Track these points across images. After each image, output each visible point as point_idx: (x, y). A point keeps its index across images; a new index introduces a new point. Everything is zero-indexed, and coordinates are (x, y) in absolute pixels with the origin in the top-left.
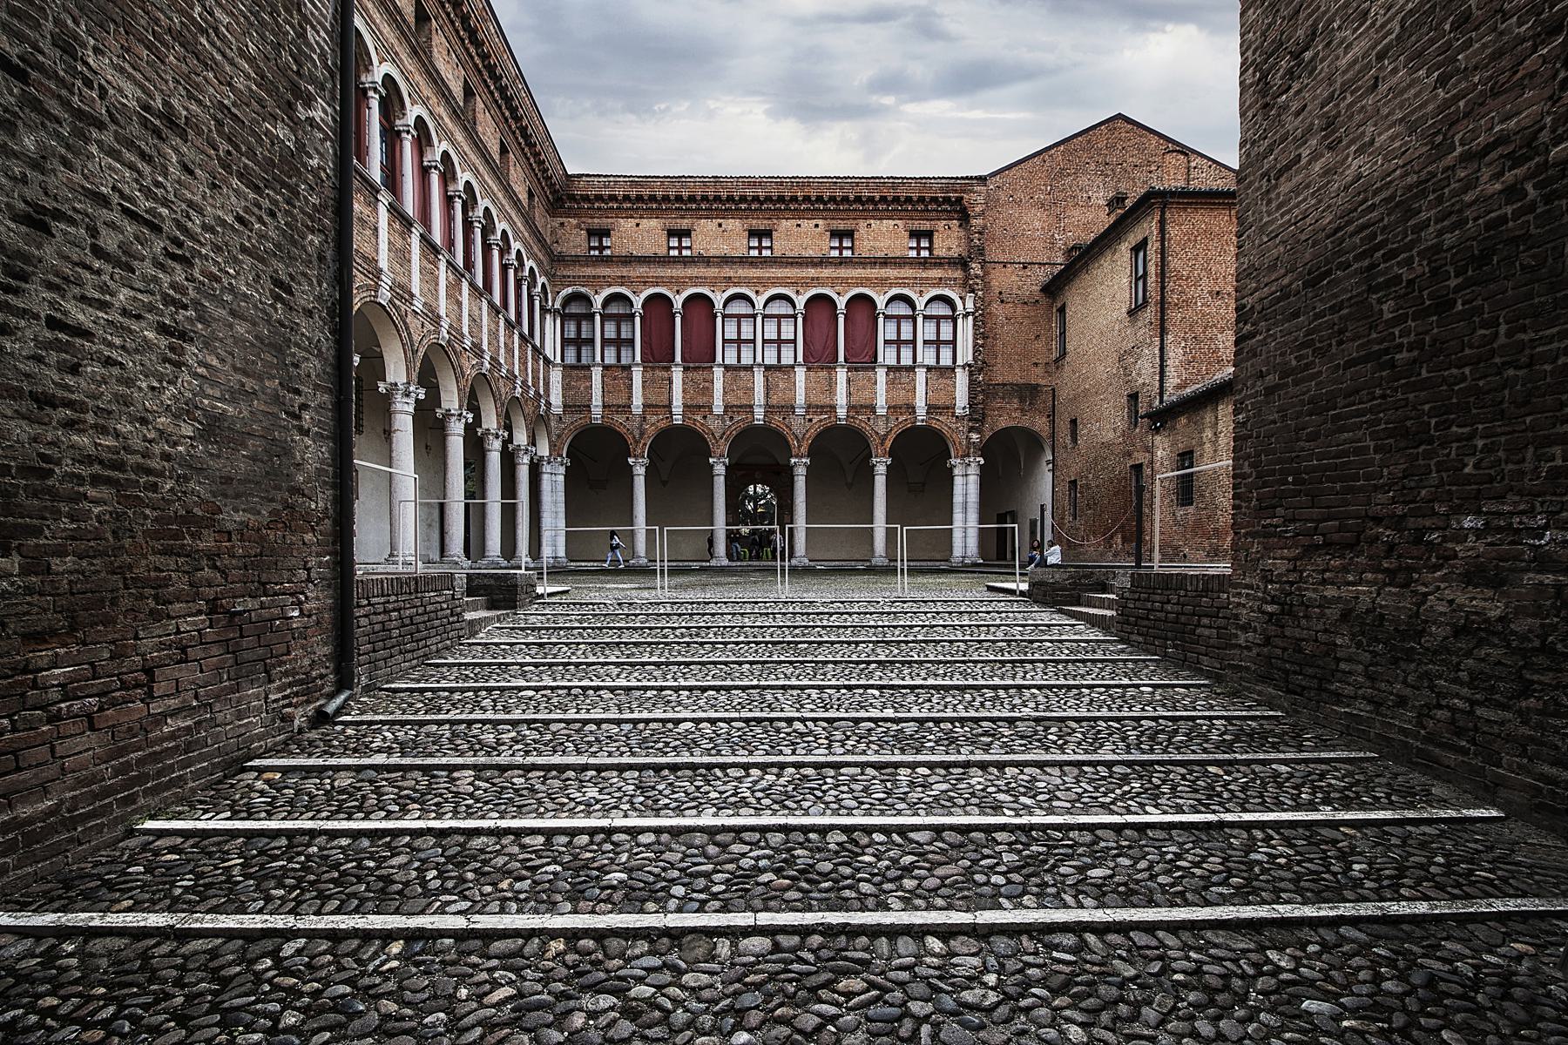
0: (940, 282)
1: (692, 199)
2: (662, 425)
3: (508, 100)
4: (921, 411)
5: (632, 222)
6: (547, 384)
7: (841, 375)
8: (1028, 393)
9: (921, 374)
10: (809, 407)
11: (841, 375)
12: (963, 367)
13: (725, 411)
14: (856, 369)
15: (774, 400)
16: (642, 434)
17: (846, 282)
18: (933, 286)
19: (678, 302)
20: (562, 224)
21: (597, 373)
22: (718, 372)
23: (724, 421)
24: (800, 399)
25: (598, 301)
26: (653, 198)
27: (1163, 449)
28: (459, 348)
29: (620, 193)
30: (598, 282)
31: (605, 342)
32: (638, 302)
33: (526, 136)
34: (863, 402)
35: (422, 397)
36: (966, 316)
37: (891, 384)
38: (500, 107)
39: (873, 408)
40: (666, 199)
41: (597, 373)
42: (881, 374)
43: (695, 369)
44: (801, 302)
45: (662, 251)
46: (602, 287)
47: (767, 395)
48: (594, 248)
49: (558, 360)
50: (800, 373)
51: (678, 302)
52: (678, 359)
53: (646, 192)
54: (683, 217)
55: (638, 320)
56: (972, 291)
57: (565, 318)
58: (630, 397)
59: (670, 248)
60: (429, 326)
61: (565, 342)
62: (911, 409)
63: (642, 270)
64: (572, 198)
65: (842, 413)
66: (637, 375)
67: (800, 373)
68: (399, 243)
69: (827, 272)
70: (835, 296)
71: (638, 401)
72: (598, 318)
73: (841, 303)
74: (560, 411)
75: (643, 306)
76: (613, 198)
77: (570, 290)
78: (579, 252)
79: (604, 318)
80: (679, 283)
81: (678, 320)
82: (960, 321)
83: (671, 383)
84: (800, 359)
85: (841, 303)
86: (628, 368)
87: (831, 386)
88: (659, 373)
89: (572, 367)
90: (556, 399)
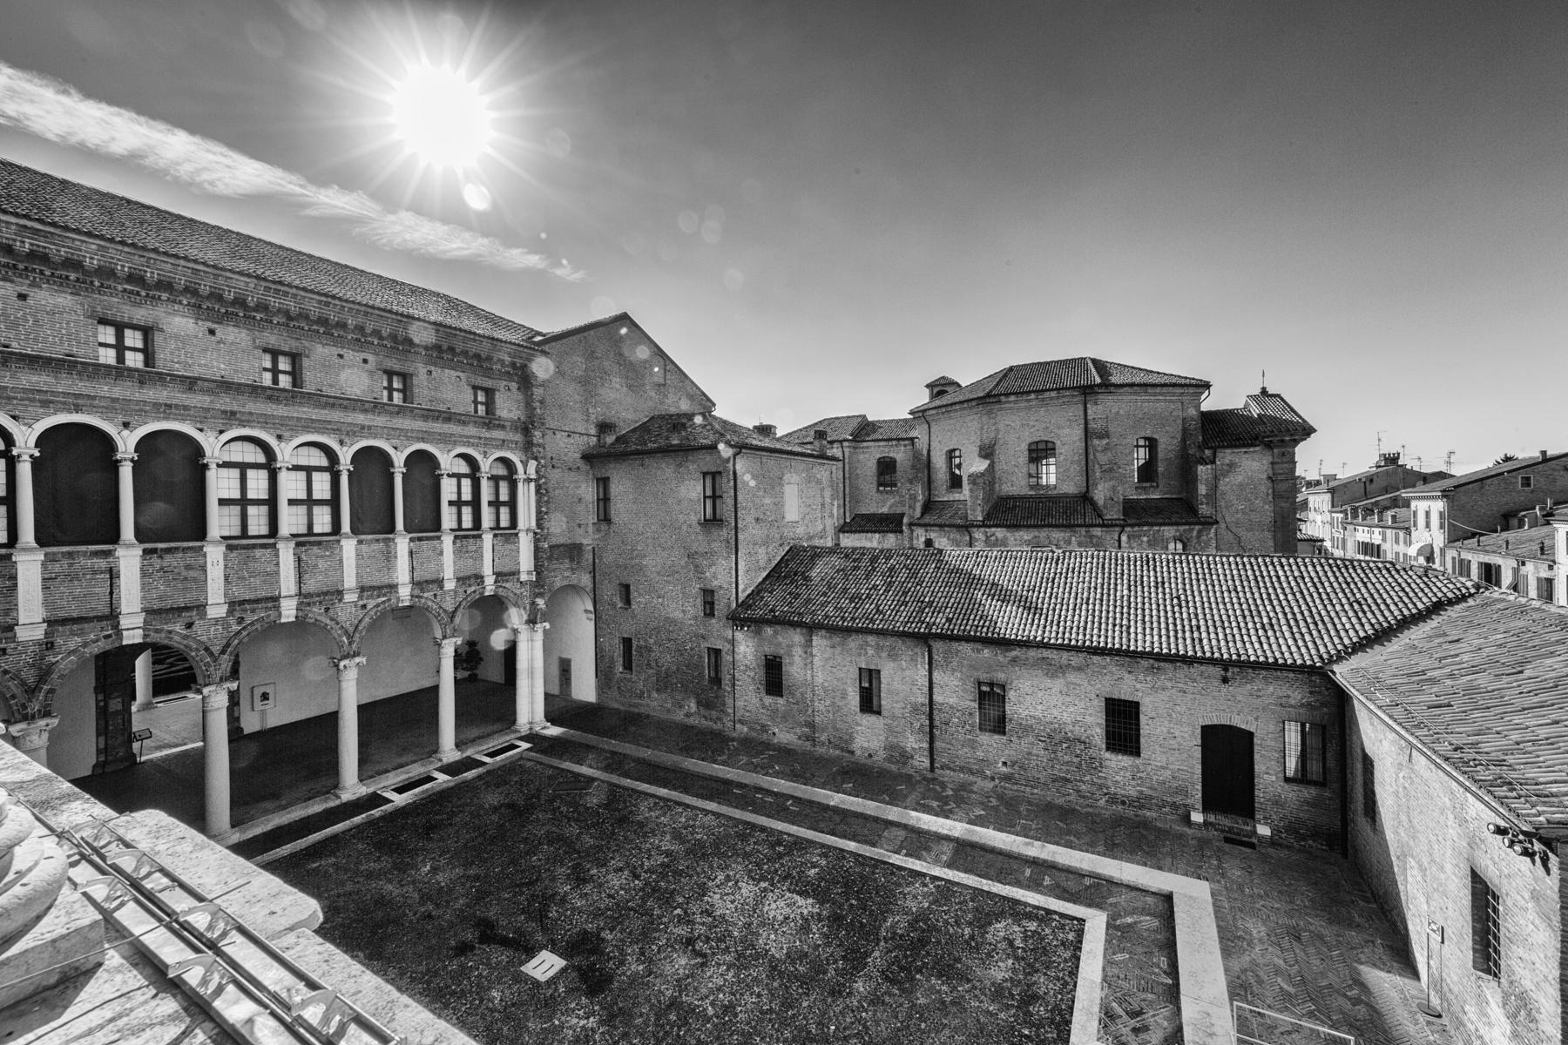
0: (503, 444)
4: (489, 581)
7: (402, 544)
8: (573, 551)
9: (488, 539)
10: (362, 589)
11: (402, 544)
12: (528, 530)
13: (230, 612)
14: (420, 539)
15: (311, 585)
17: (408, 436)
18: (497, 447)
22: (214, 555)
23: (227, 626)
24: (350, 581)
27: (746, 649)
34: (428, 577)
36: (529, 480)
37: (458, 553)
39: (439, 582)
42: (447, 541)
43: (169, 551)
44: (345, 456)
47: (300, 581)
50: (349, 546)
51: (127, 443)
56: (536, 459)
62: (479, 578)
65: (405, 592)
67: (349, 546)
69: (380, 420)
70: (391, 451)
73: (399, 459)
75: (39, 443)
81: (126, 474)
82: (520, 485)
83: (113, 574)
84: (346, 526)
85: (399, 459)
87: (389, 557)
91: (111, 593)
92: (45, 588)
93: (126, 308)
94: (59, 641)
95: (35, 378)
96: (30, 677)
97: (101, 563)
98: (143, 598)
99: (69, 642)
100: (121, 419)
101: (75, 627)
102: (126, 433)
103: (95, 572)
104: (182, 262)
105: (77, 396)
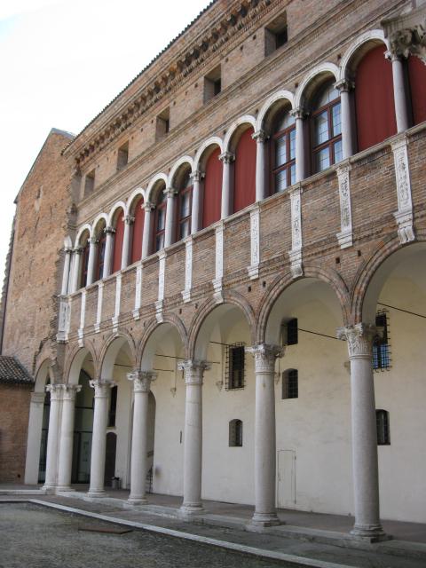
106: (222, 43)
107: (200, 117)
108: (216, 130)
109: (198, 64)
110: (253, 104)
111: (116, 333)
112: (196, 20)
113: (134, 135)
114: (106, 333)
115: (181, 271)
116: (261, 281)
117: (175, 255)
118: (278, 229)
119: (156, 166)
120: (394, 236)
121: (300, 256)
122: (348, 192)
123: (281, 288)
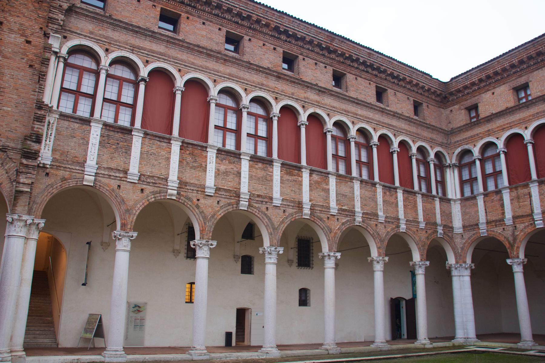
1: (521, 62)
2: (529, 230)
3: (371, 66)
5: (489, 93)
6: (447, 215)
16: (515, 239)
19: (527, 135)
20: (451, 111)
21: (480, 201)
25: (476, 151)
26: (496, 74)
28: (323, 216)
29: (475, 79)
30: (473, 140)
31: (485, 177)
32: (500, 144)
33: (394, 77)
35: (281, 252)
38: (367, 72)
40: (504, 70)
41: (480, 201)
45: (511, 104)
46: (477, 141)
48: (474, 117)
49: (459, 196)
51: (527, 135)
52: (534, 176)
53: (490, 72)
54: (520, 76)
55: (502, 156)
57: (460, 167)
58: (503, 213)
59: (520, 99)
60: (290, 211)
61: (462, 183)
63: (500, 122)
64: (451, 94)
66: (506, 196)
68: (261, 173)
71: (509, 215)
72: (478, 163)
74: (461, 231)
76: (473, 84)
77: (459, 150)
78: (462, 123)
79: (483, 161)
80: (524, 123)
81: (530, 148)
86: (498, 192)
88: (521, 191)
89: (468, 199)
90: (457, 223)
91: (531, 204)
92: (511, 203)
93: (518, 80)
94: (518, 226)
95: (500, 121)
96: (511, 239)
97: (526, 191)
98: (541, 206)
99: (520, 226)
100: (524, 126)
101: (521, 219)
102: (526, 131)
103: (524, 195)
104: (520, 49)
105: (510, 123)
106: (308, 49)
107: (284, 79)
108: (297, 99)
109: (286, 41)
110: (327, 109)
111: (172, 195)
112: (307, 23)
113: (191, 17)
114: (149, 189)
115: (268, 180)
116: (336, 217)
117: (260, 165)
118: (346, 194)
119: (230, 75)
120: (398, 227)
121: (361, 215)
122: (381, 198)
123: (348, 226)
